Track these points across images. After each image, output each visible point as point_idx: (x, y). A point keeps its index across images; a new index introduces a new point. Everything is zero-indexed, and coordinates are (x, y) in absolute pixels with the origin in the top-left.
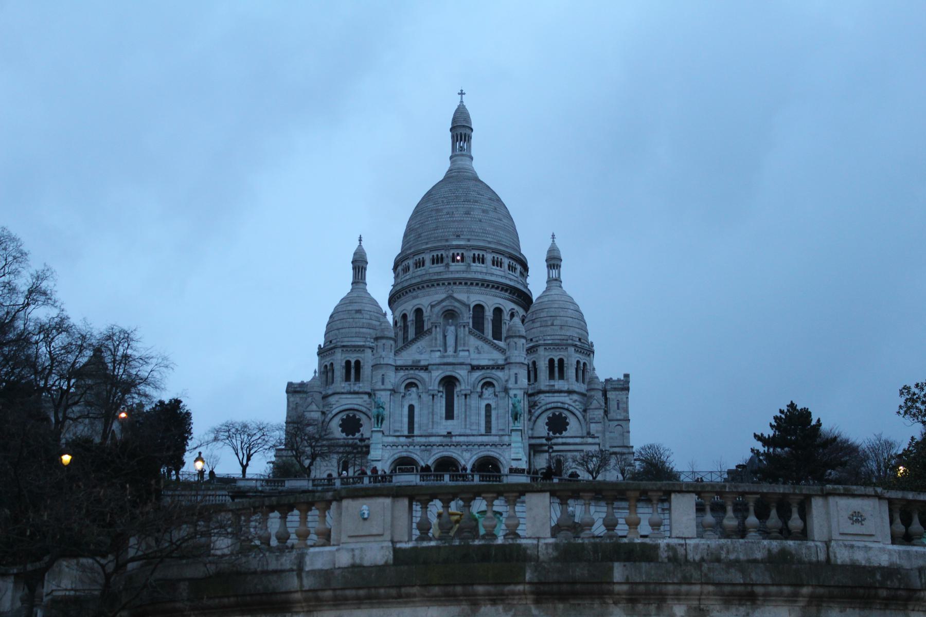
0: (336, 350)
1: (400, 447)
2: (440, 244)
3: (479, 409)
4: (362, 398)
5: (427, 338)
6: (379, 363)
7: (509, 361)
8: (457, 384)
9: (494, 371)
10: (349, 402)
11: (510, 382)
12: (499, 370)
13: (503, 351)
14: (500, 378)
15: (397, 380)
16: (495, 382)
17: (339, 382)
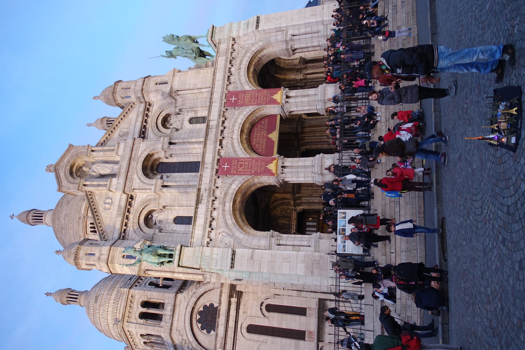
0: (126, 329)
1: (215, 214)
2: (81, 225)
3: (192, 131)
4: (181, 301)
5: (97, 198)
6: (106, 262)
7: (140, 95)
8: (156, 156)
9: (150, 114)
10: (183, 316)
11: (164, 90)
12: (151, 108)
13: (132, 105)
14: (160, 107)
15: (137, 238)
16: (163, 114)
17: (159, 329)
